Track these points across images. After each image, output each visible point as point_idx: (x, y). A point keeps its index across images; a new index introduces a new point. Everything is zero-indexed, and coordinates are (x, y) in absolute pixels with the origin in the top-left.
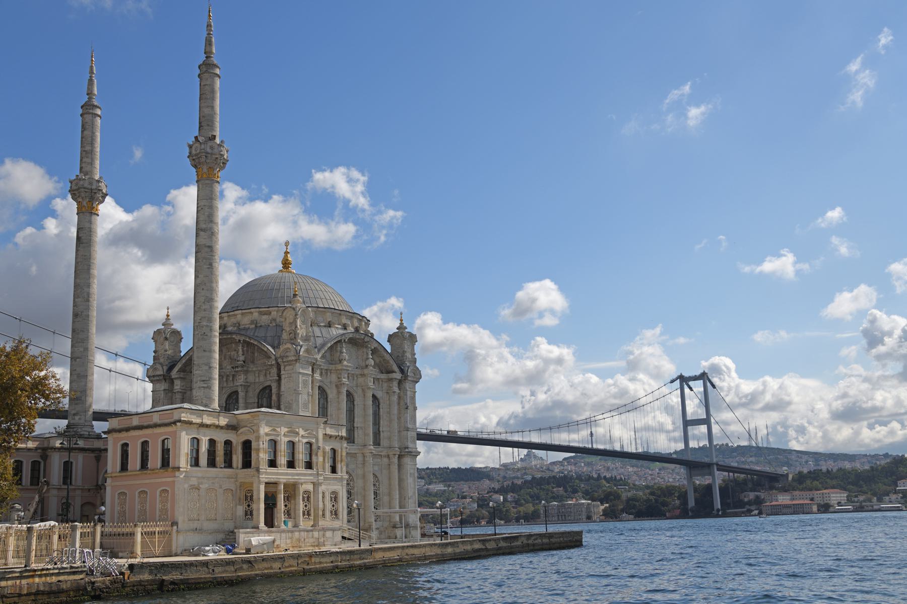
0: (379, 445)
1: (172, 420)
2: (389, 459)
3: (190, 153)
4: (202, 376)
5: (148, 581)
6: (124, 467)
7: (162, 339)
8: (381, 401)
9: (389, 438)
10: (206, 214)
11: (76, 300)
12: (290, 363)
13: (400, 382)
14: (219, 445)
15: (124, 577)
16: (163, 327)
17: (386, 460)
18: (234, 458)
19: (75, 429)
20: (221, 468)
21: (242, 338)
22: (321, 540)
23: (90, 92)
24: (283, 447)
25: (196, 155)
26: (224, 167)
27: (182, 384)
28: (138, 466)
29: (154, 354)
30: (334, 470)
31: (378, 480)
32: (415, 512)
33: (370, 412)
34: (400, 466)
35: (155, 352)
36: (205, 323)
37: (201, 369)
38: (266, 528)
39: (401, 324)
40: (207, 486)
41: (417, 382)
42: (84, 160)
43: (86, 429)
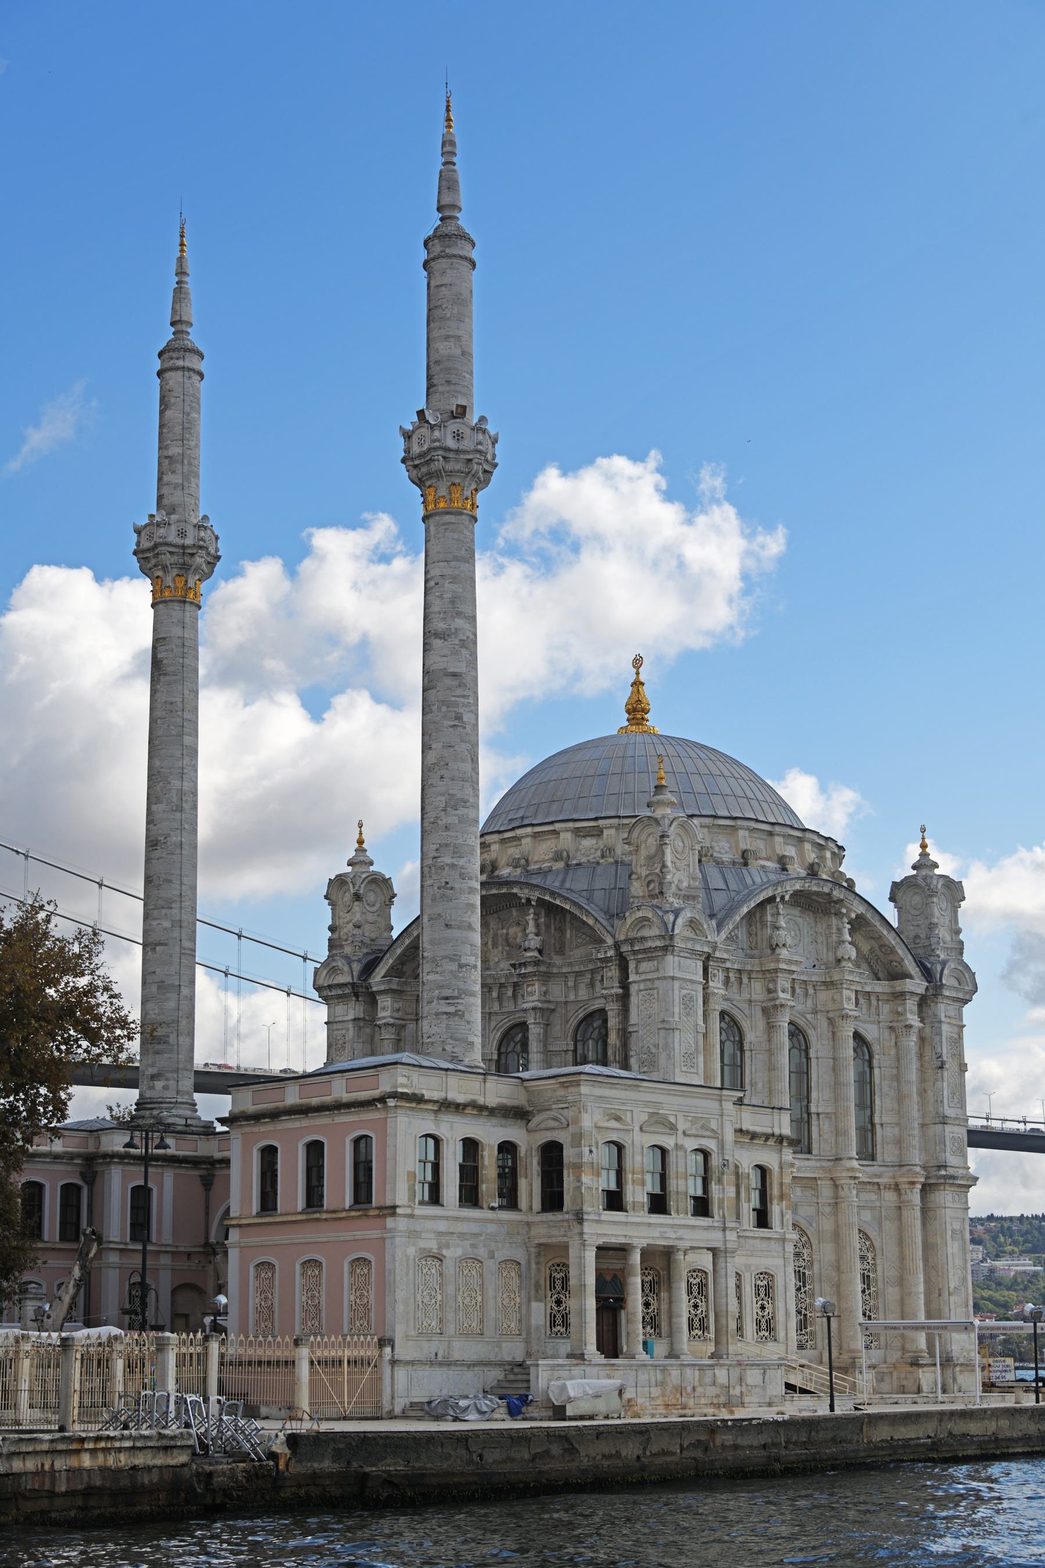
0: (873, 1158)
1: (376, 1093)
2: (900, 1195)
3: (407, 451)
4: (441, 987)
5: (331, 1475)
6: (268, 1201)
7: (348, 897)
8: (876, 1048)
9: (899, 1142)
10: (448, 595)
11: (154, 807)
12: (651, 954)
13: (923, 1002)
14: (486, 1153)
15: (277, 1465)
16: (349, 869)
17: (890, 1196)
18: (523, 1184)
19: (155, 1112)
20: (493, 1209)
21: (535, 895)
22: (736, 1391)
23: (177, 318)
25: (421, 456)
26: (487, 482)
27: (396, 1006)
28: (301, 1203)
29: (329, 934)
30: (762, 1219)
31: (872, 1245)
32: (967, 1327)
33: (850, 1075)
34: (926, 1212)
35: (332, 929)
36: (448, 860)
37: (439, 969)
38: (600, 1359)
40: (459, 1252)
41: (966, 1002)
42: (166, 478)
43: (180, 1112)
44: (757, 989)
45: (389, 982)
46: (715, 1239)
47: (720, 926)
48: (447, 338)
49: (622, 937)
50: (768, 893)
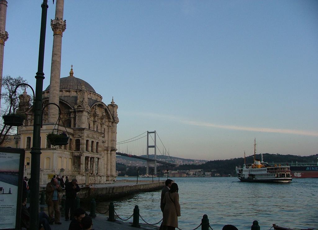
13: (112, 123)
17: (106, 152)
22: (100, 180)
24: (90, 143)
25: (54, 24)
45: (30, 113)
46: (98, 156)
47: (90, 108)
48: (60, 6)
49: (76, 108)
50: (96, 104)
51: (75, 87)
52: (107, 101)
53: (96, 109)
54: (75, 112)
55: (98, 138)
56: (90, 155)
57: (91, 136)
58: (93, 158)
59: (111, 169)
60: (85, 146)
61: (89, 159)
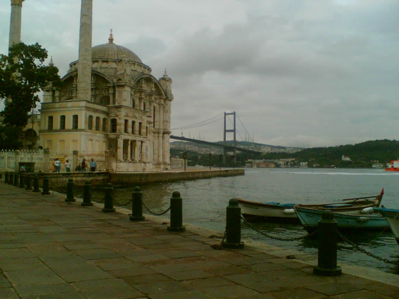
4: (83, 87)
8: (156, 108)
13: (165, 100)
17: (156, 135)
24: (130, 123)
28: (59, 128)
38: (123, 161)
39: (165, 73)
41: (171, 101)
44: (138, 95)
46: (142, 139)
49: (115, 82)
50: (142, 77)
51: (115, 56)
52: (157, 74)
53: (142, 84)
54: (114, 87)
55: (142, 118)
56: (130, 137)
57: (131, 114)
58: (135, 141)
59: (164, 156)
60: (123, 127)
61: (130, 142)
